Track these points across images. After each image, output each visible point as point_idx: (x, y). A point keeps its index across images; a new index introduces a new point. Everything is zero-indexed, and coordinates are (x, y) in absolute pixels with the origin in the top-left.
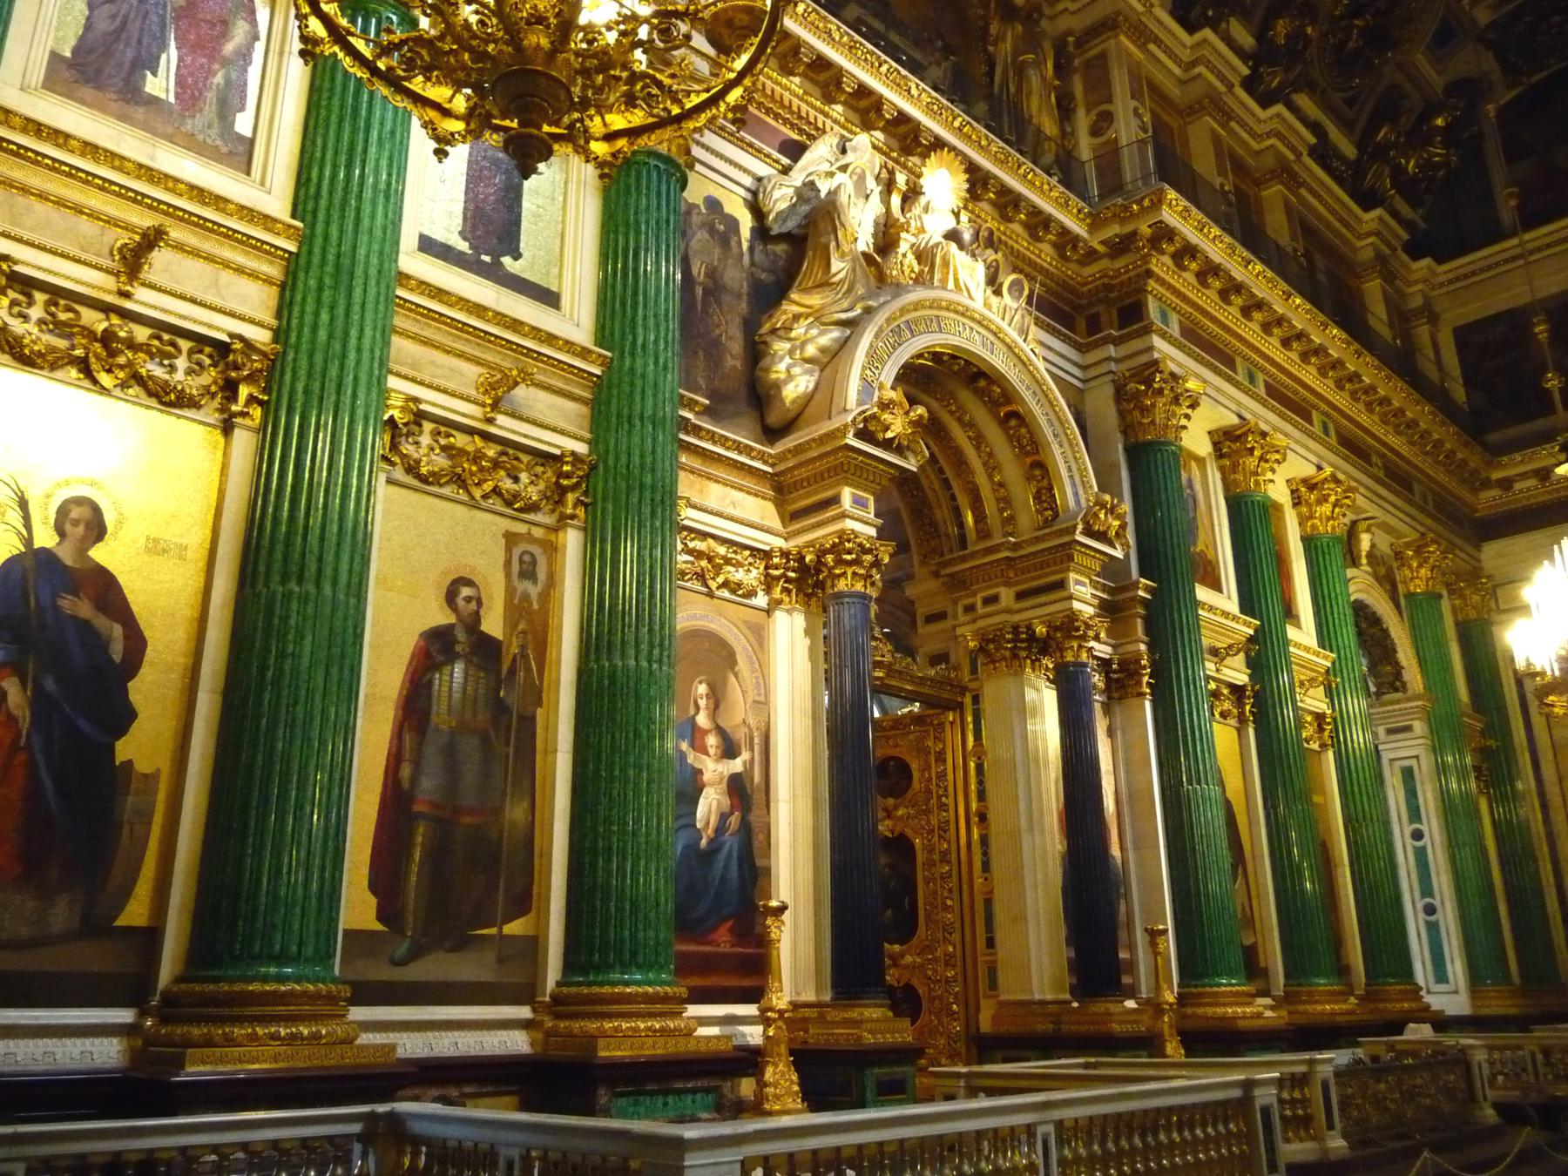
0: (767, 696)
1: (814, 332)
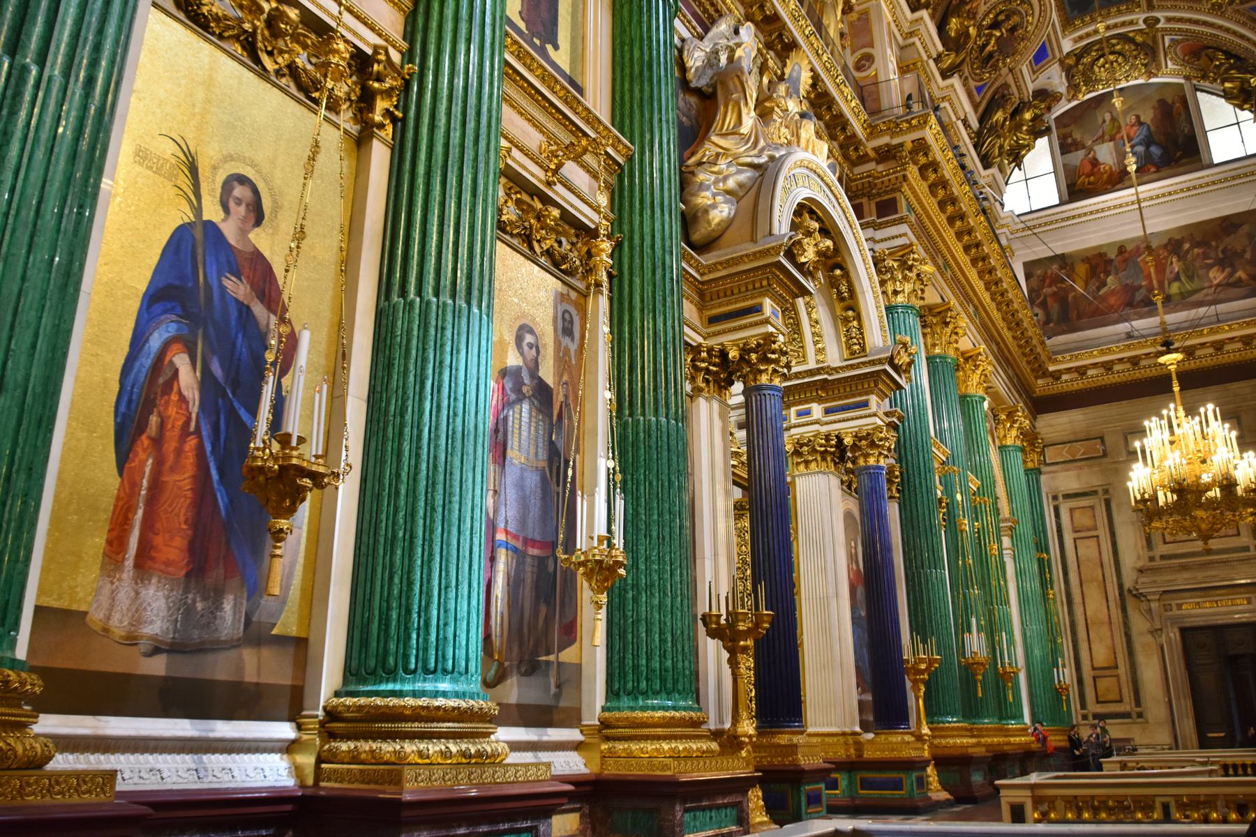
1: (733, 169)
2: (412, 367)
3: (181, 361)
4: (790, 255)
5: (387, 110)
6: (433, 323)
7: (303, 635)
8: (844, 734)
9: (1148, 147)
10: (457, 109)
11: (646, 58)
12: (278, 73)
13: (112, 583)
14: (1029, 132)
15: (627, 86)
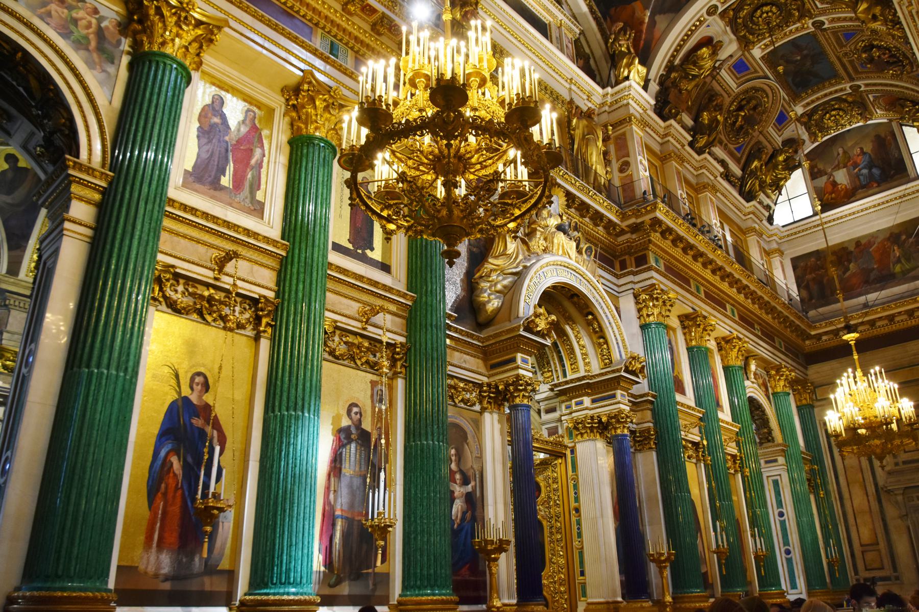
0: (481, 454)
1: (500, 278)
3: (174, 460)
4: (528, 329)
8: (607, 603)
9: (870, 169)
12: (214, 320)
14: (784, 169)
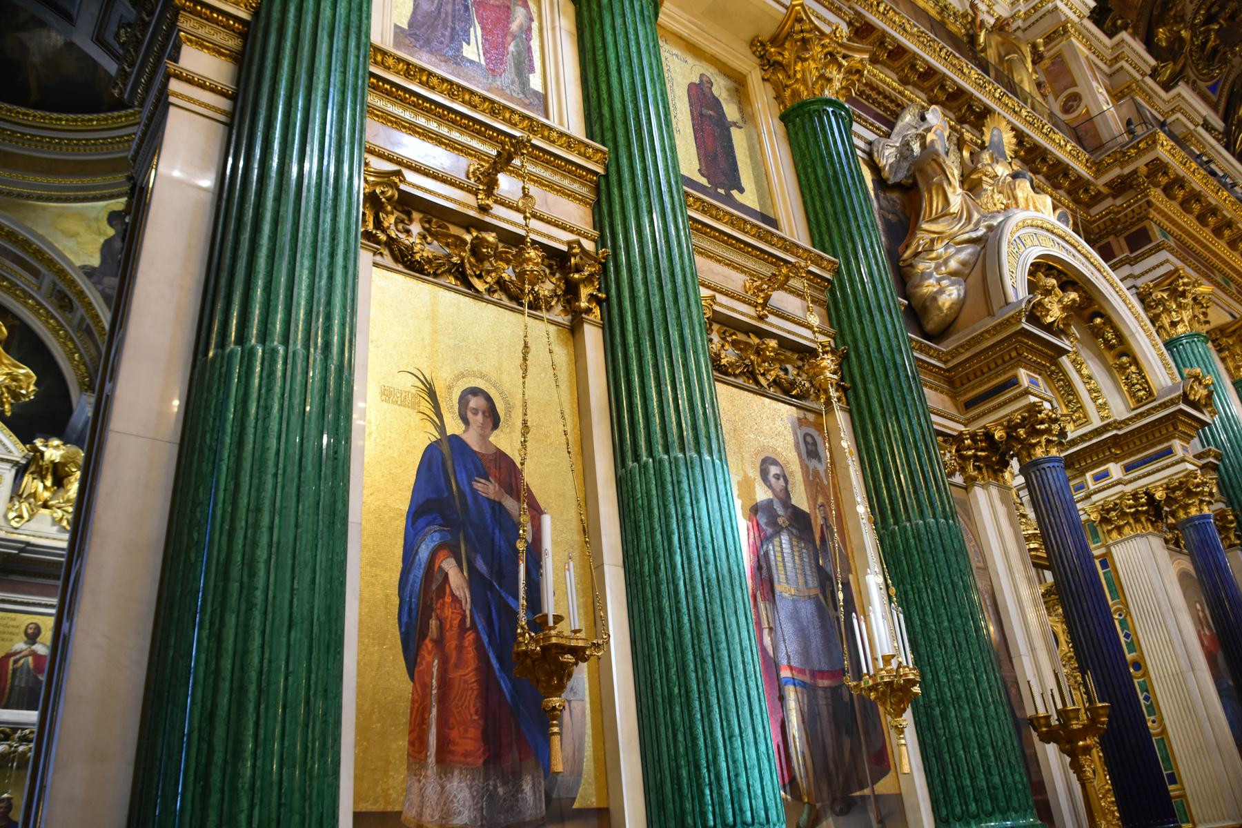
0: (985, 561)
1: (952, 250)
2: (657, 526)
3: (449, 565)
4: (1034, 319)
5: (591, 295)
6: (669, 479)
7: (604, 805)
10: (652, 276)
11: (830, 173)
12: (490, 291)
13: (419, 781)
15: (818, 204)
